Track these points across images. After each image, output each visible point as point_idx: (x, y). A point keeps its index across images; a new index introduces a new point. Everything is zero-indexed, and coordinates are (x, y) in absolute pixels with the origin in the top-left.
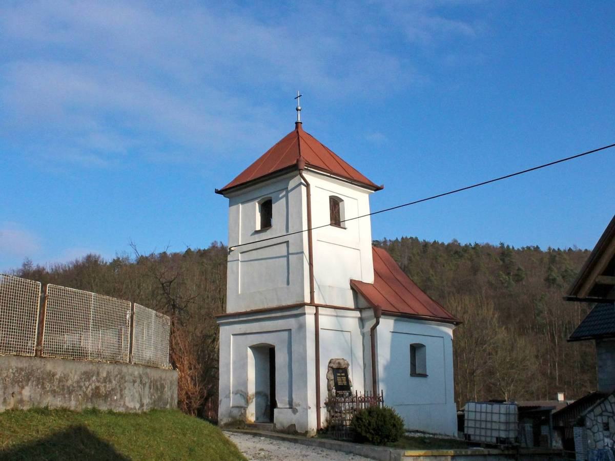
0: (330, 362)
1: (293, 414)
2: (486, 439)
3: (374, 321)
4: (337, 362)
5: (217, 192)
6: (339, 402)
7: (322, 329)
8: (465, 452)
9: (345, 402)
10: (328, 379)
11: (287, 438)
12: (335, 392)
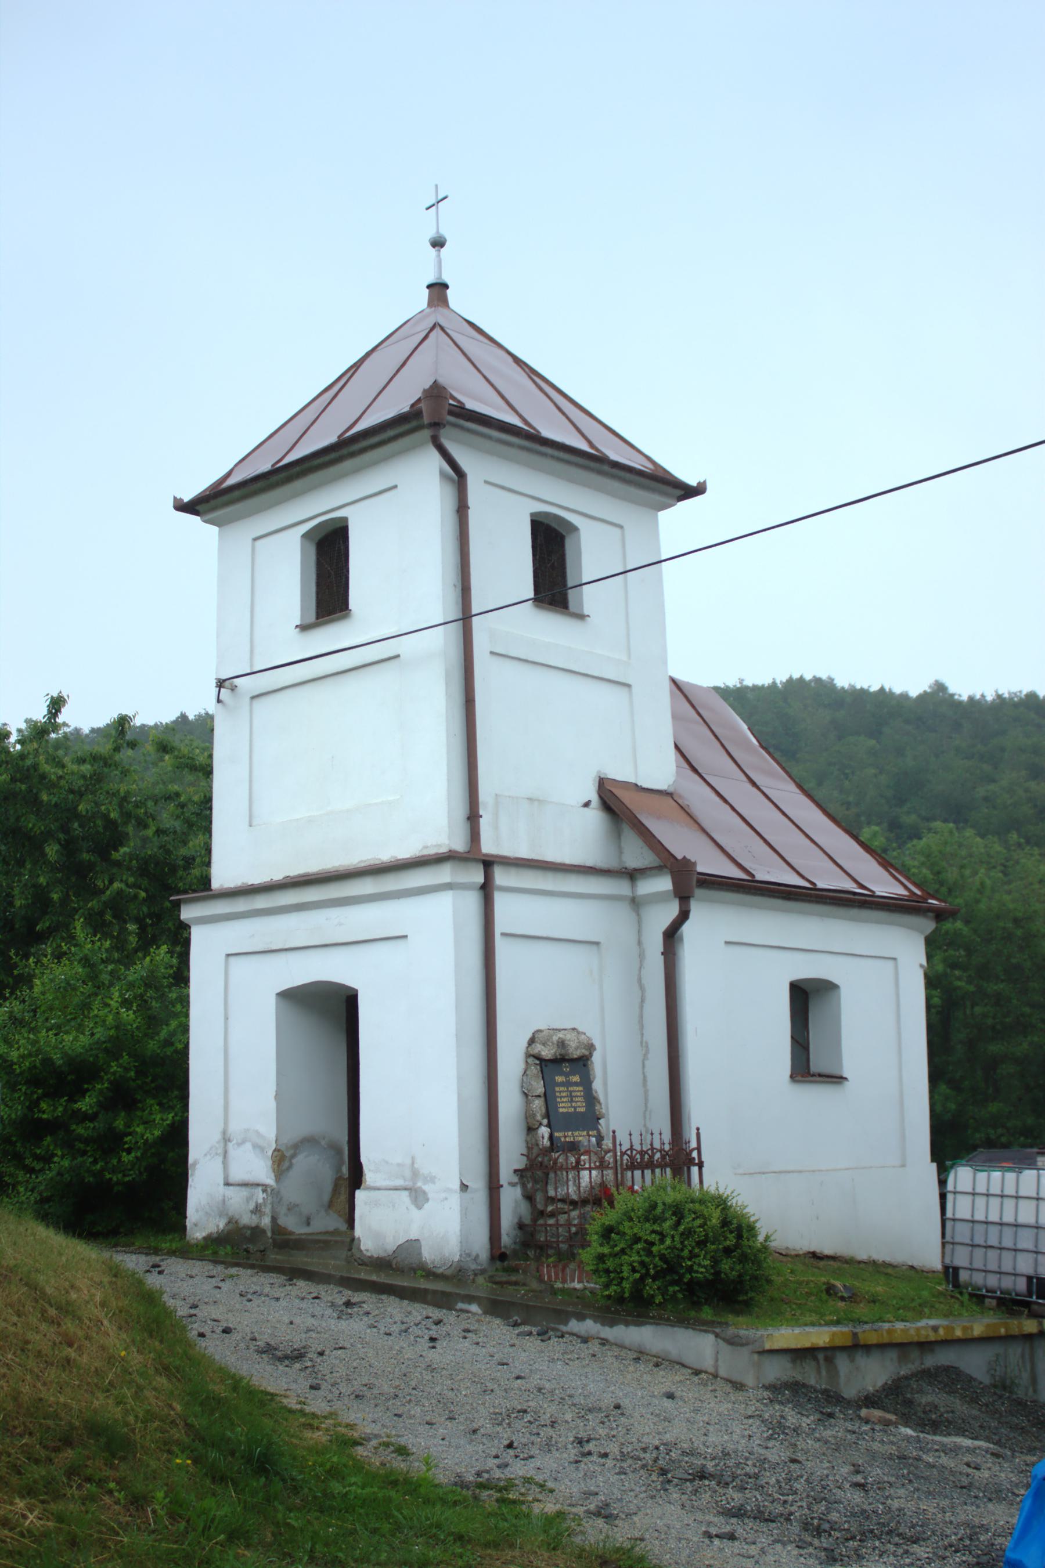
0: (532, 1041)
1: (412, 1207)
2: (971, 1276)
3: (673, 910)
4: (555, 1038)
5: (182, 507)
6: (561, 1168)
7: (503, 934)
8: (965, 1329)
9: (578, 1167)
10: (526, 1095)
11: (391, 1285)
12: (546, 1136)
